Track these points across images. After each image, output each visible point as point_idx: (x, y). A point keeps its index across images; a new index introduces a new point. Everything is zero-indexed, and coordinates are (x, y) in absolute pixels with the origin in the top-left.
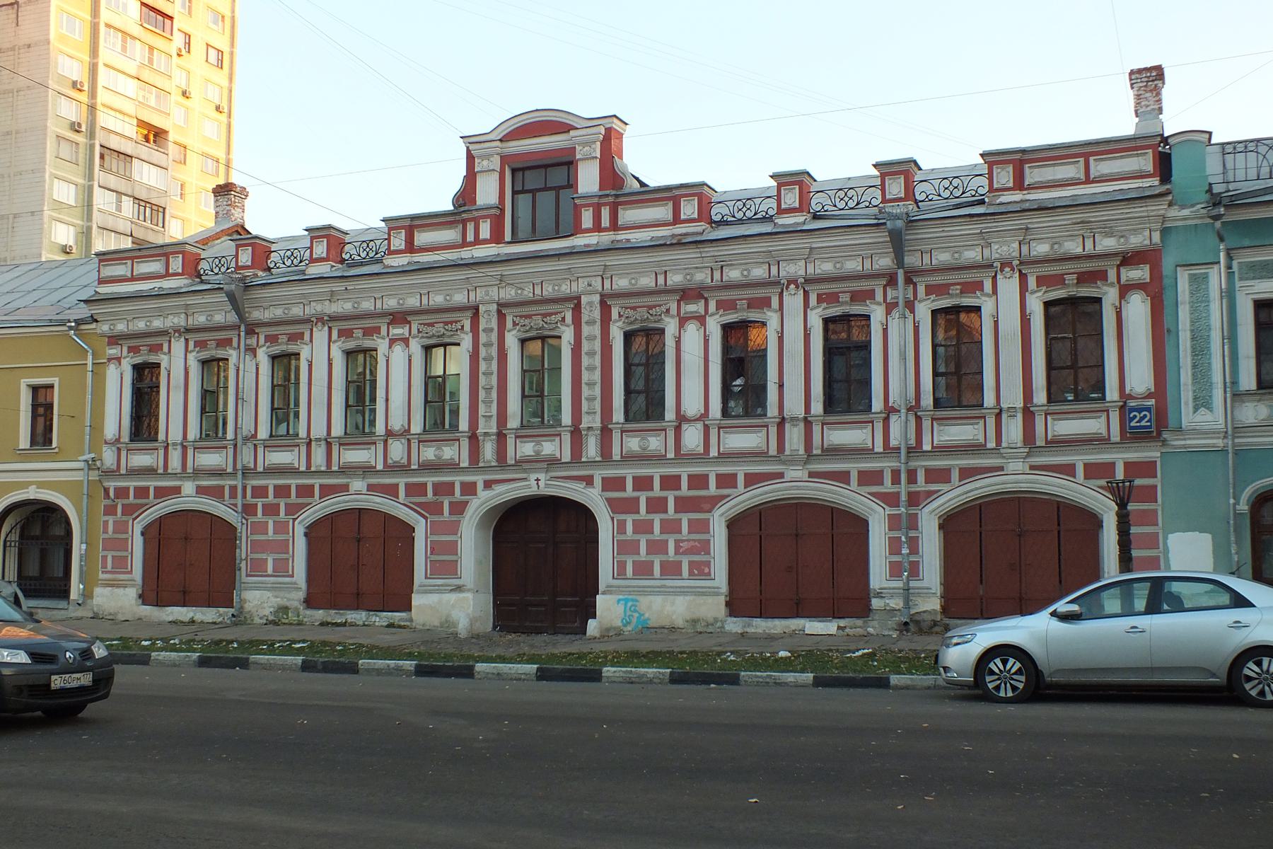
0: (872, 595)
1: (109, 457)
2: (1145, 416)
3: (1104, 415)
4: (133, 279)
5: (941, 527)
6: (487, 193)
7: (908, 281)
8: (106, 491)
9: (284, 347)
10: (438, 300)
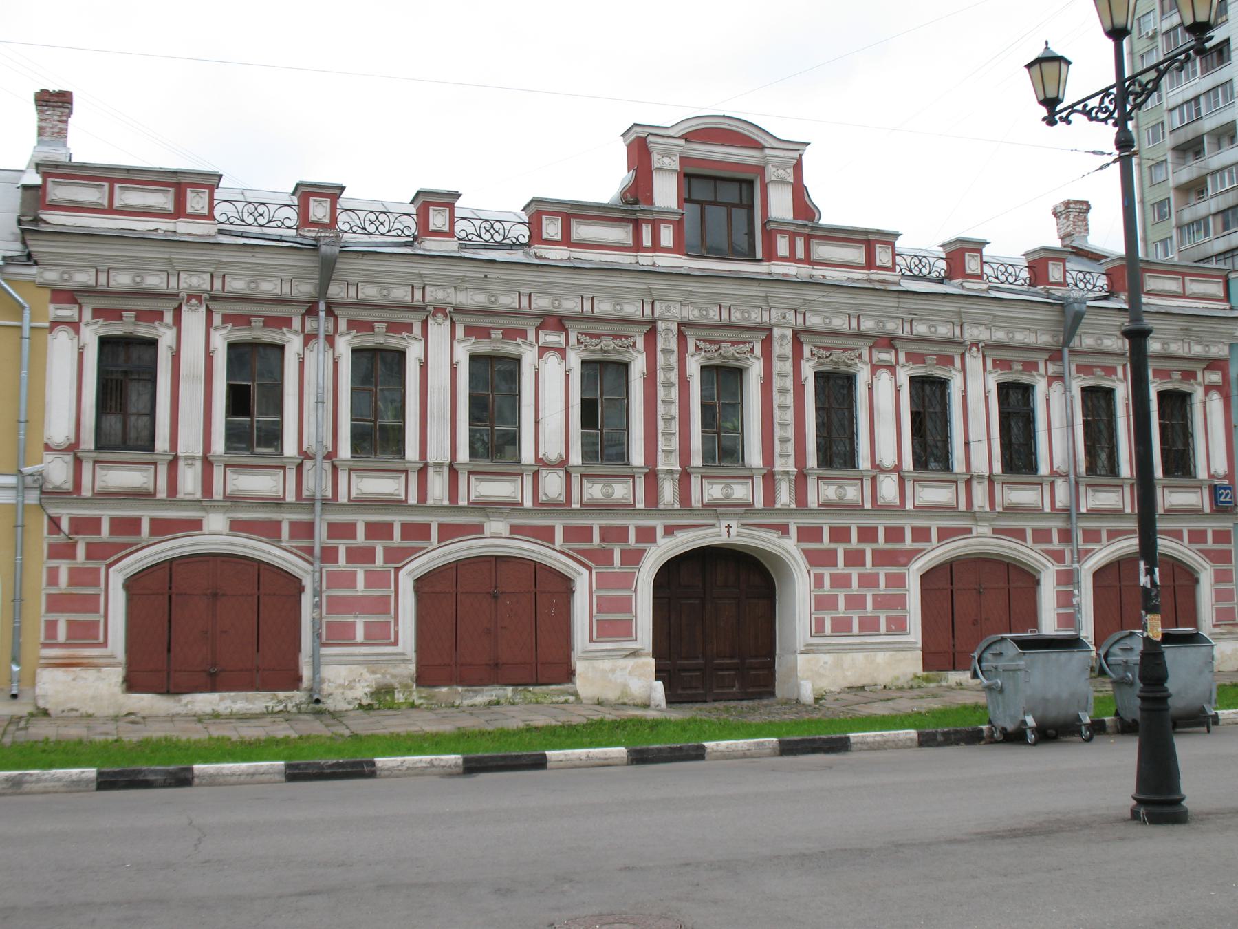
1: (58, 472)
4: (110, 210)
6: (666, 193)
8: (55, 523)
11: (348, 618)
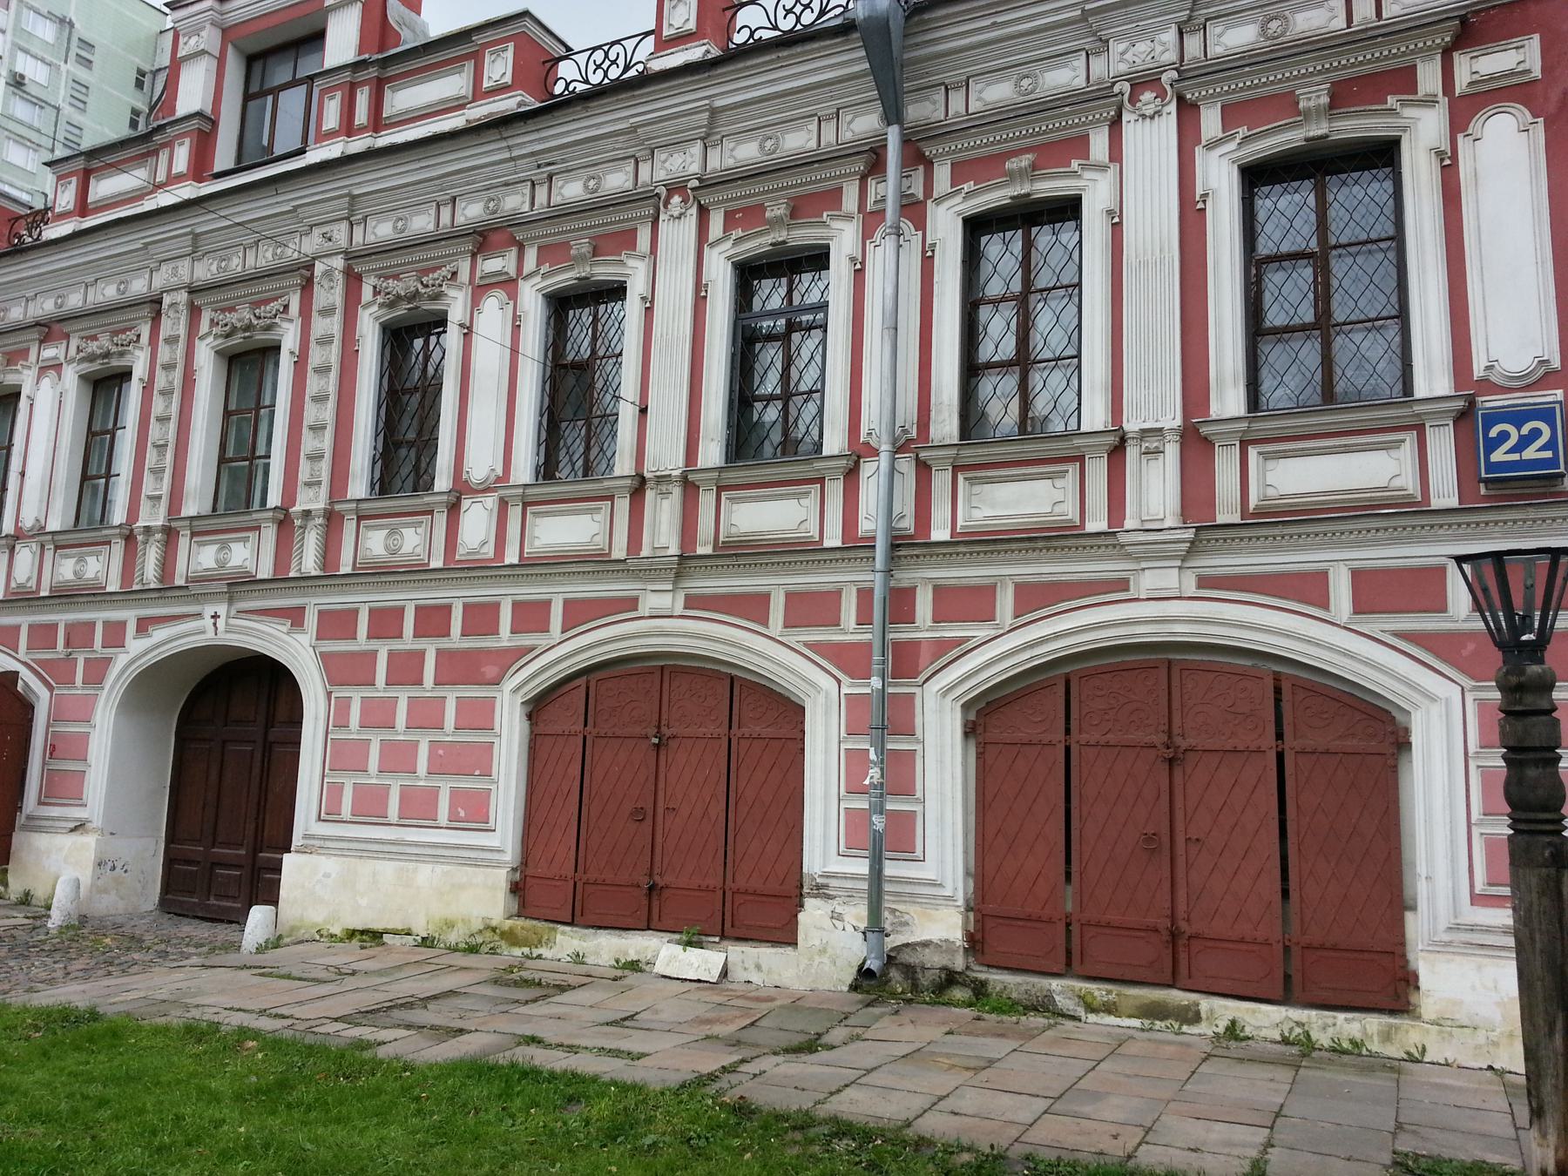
0: (806, 890)
2: (1536, 433)
3: (1410, 438)
5: (970, 731)
7: (916, 156)
10: (108, 292)
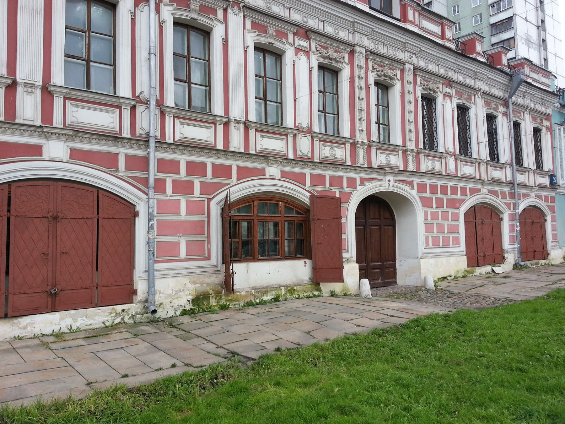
9: (195, 16)
11: (175, 239)
